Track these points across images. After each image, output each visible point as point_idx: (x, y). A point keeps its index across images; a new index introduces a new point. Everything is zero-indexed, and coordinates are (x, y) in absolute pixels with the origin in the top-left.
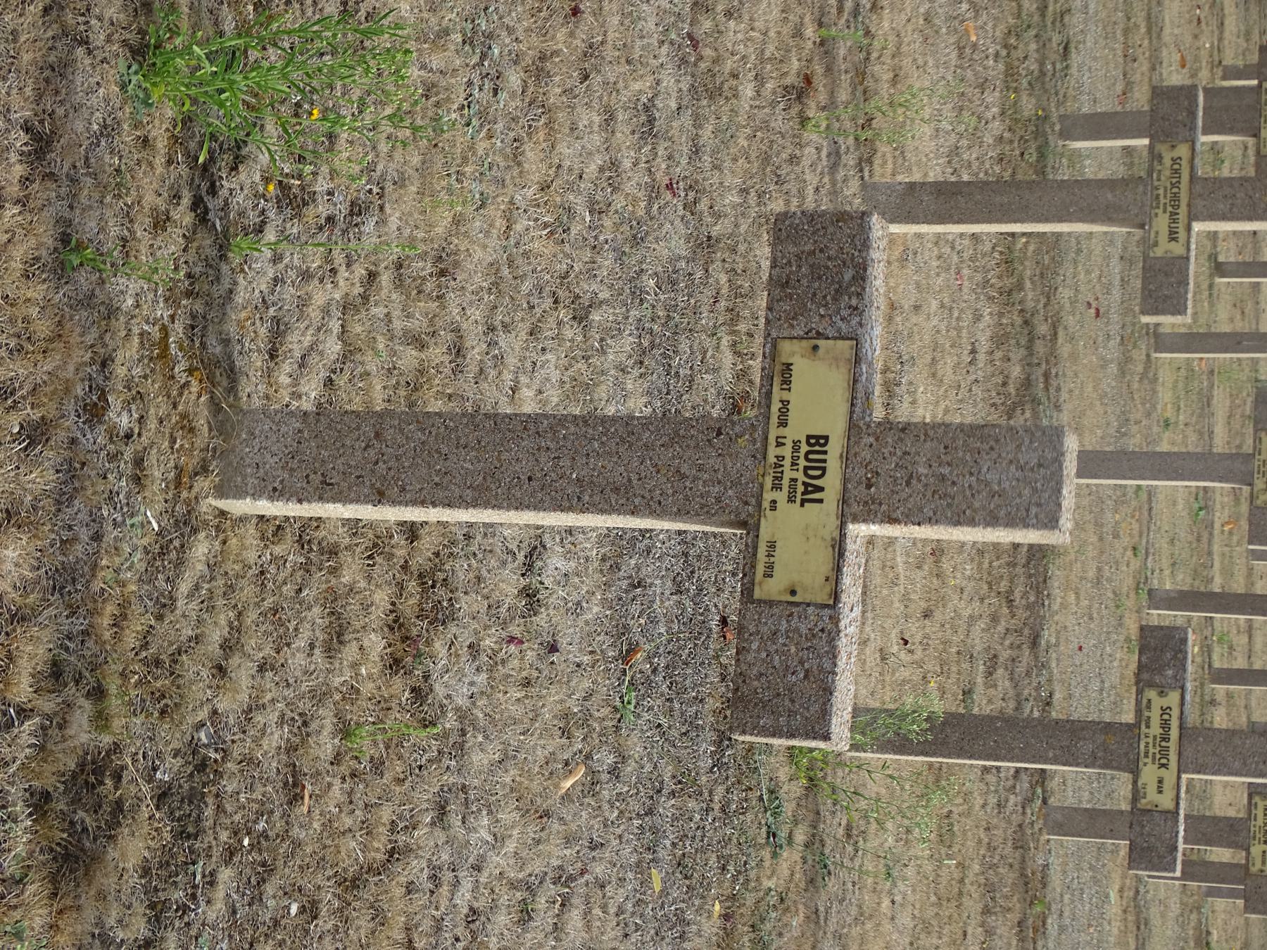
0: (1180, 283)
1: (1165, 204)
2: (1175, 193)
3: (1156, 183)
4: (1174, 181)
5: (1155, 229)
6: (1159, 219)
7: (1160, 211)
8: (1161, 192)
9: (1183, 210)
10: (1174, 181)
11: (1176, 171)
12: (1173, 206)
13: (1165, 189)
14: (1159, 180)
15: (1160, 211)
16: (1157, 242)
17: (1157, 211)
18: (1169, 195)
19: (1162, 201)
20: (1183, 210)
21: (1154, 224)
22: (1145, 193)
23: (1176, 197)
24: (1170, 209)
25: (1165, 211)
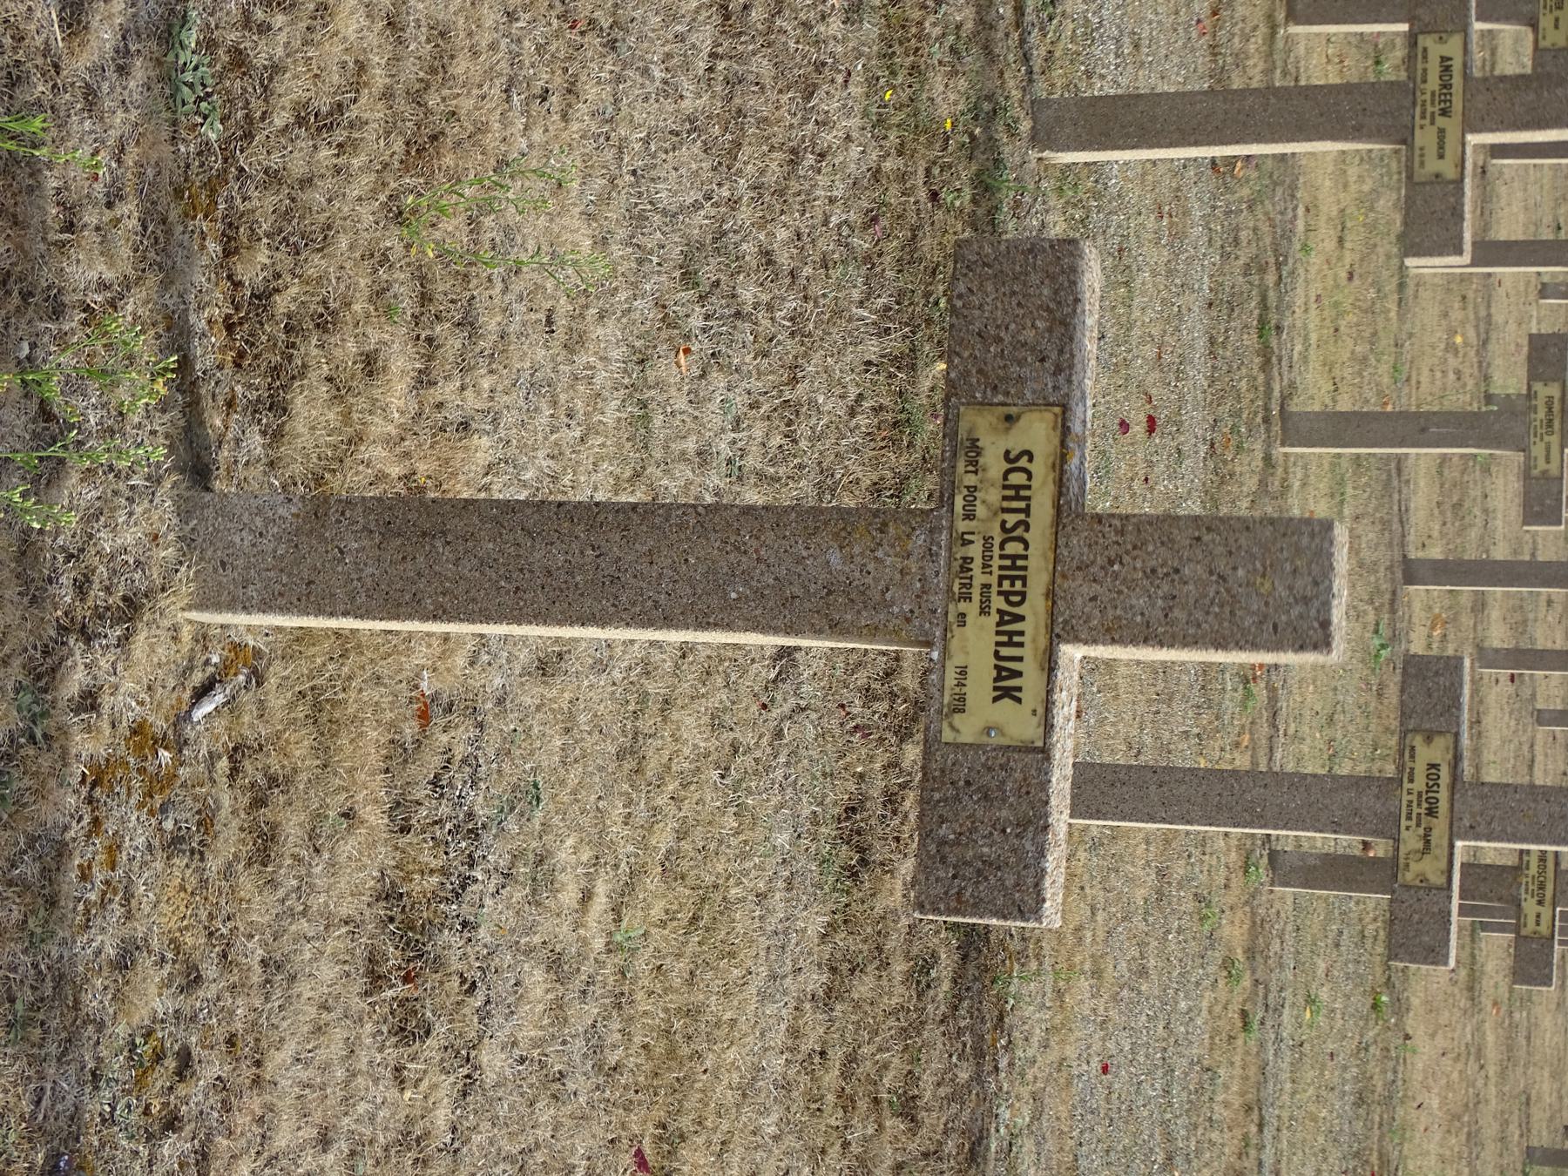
0: (1023, 824)
1: (987, 586)
2: (1014, 558)
3: (962, 526)
4: (1012, 519)
5: (957, 660)
6: (969, 630)
7: (971, 609)
8: (975, 550)
9: (1034, 609)
10: (1012, 519)
11: (1018, 493)
12: (1006, 595)
13: (987, 540)
14: (970, 516)
15: (971, 609)
16: (962, 699)
17: (963, 606)
18: (996, 562)
19: (979, 578)
20: (1034, 609)
21: (954, 644)
22: (932, 555)
23: (1015, 570)
24: (998, 602)
25: (984, 611)
